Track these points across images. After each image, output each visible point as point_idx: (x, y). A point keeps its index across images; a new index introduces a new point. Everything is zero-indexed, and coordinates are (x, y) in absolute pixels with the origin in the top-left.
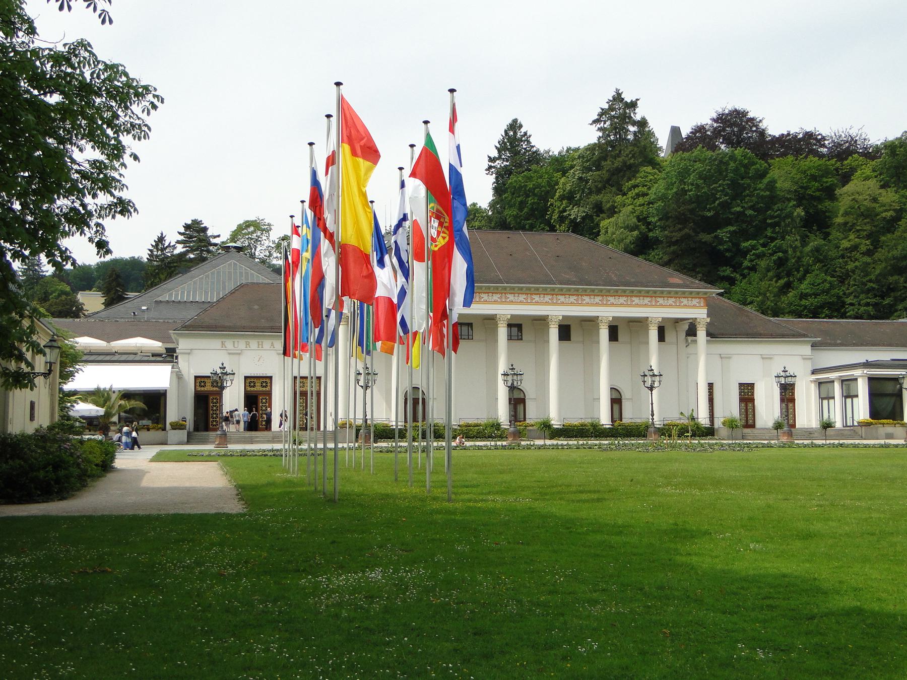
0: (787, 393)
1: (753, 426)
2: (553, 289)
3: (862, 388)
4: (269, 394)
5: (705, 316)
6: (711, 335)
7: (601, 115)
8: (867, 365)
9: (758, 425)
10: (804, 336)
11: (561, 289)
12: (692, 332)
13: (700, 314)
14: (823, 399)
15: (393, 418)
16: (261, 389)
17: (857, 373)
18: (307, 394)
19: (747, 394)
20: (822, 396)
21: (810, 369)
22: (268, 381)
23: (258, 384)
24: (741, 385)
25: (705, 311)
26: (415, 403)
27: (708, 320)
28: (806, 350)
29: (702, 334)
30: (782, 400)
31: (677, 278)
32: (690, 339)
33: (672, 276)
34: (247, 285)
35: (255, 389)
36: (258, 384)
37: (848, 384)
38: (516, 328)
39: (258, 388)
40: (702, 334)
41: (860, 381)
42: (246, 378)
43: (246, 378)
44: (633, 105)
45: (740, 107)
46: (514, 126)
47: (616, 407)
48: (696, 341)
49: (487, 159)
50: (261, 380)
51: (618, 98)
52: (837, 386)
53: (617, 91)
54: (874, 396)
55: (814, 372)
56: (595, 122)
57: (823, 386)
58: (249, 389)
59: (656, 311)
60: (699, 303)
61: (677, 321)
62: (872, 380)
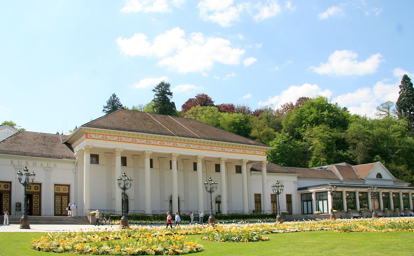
4: (40, 194)
14: (303, 201)
16: (34, 191)
18: (63, 195)
20: (303, 200)
21: (297, 188)
22: (39, 186)
29: (264, 169)
35: (31, 190)
36: (33, 187)
39: (33, 190)
40: (264, 169)
45: (205, 93)
49: (103, 106)
50: (35, 185)
57: (302, 195)
58: (27, 190)
60: (263, 154)
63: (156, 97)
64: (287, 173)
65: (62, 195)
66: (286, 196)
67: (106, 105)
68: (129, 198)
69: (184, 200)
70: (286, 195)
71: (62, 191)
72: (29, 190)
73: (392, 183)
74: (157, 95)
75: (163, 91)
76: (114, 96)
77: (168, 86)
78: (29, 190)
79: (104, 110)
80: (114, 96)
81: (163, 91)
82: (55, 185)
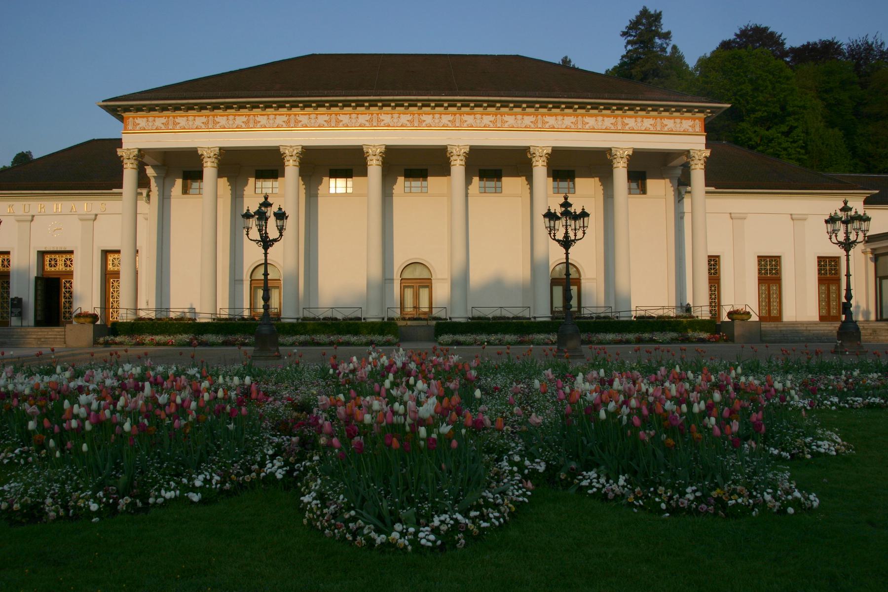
4: (70, 274)
5: (703, 147)
7: (629, 28)
19: (770, 271)
20: (880, 274)
24: (761, 259)
25: (703, 139)
27: (708, 153)
29: (698, 175)
30: (821, 281)
32: (682, 189)
39: (61, 267)
40: (698, 175)
46: (566, 57)
47: (388, 277)
50: (64, 257)
51: (644, 13)
53: (645, 7)
56: (624, 34)
60: (693, 127)
63: (629, 47)
66: (709, 261)
69: (595, 277)
70: (759, 257)
72: (53, 269)
75: (645, 29)
77: (658, 17)
78: (53, 269)
81: (645, 29)
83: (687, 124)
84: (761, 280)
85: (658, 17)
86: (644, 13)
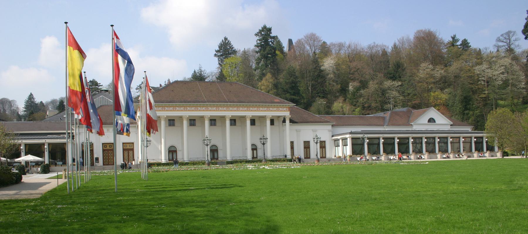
0: (323, 145)
1: (309, 158)
2: (227, 105)
3: (349, 142)
6: (292, 121)
8: (351, 133)
9: (219, 159)
10: (329, 122)
11: (230, 105)
12: (284, 121)
13: (287, 114)
15: (163, 158)
17: (347, 136)
18: (129, 150)
21: (331, 135)
23: (108, 146)
24: (304, 142)
25: (289, 113)
26: (172, 151)
28: (330, 127)
29: (288, 121)
31: (278, 99)
32: (284, 124)
33: (276, 99)
34: (103, 106)
36: (108, 146)
37: (345, 139)
38: (213, 121)
40: (288, 121)
41: (348, 139)
42: (103, 144)
43: (103, 144)
44: (270, 30)
48: (285, 125)
51: (265, 27)
52: (341, 141)
54: (353, 145)
55: (333, 136)
59: (270, 113)
61: (279, 117)
62: (353, 139)
63: (259, 42)
64: (323, 122)
65: (128, 150)
67: (218, 49)
68: (178, 149)
71: (128, 147)
73: (448, 128)
74: (260, 40)
76: (226, 39)
79: (215, 55)
80: (226, 39)
82: (123, 143)
83: (285, 109)
84: (305, 148)
85: (270, 30)
86: (265, 27)
